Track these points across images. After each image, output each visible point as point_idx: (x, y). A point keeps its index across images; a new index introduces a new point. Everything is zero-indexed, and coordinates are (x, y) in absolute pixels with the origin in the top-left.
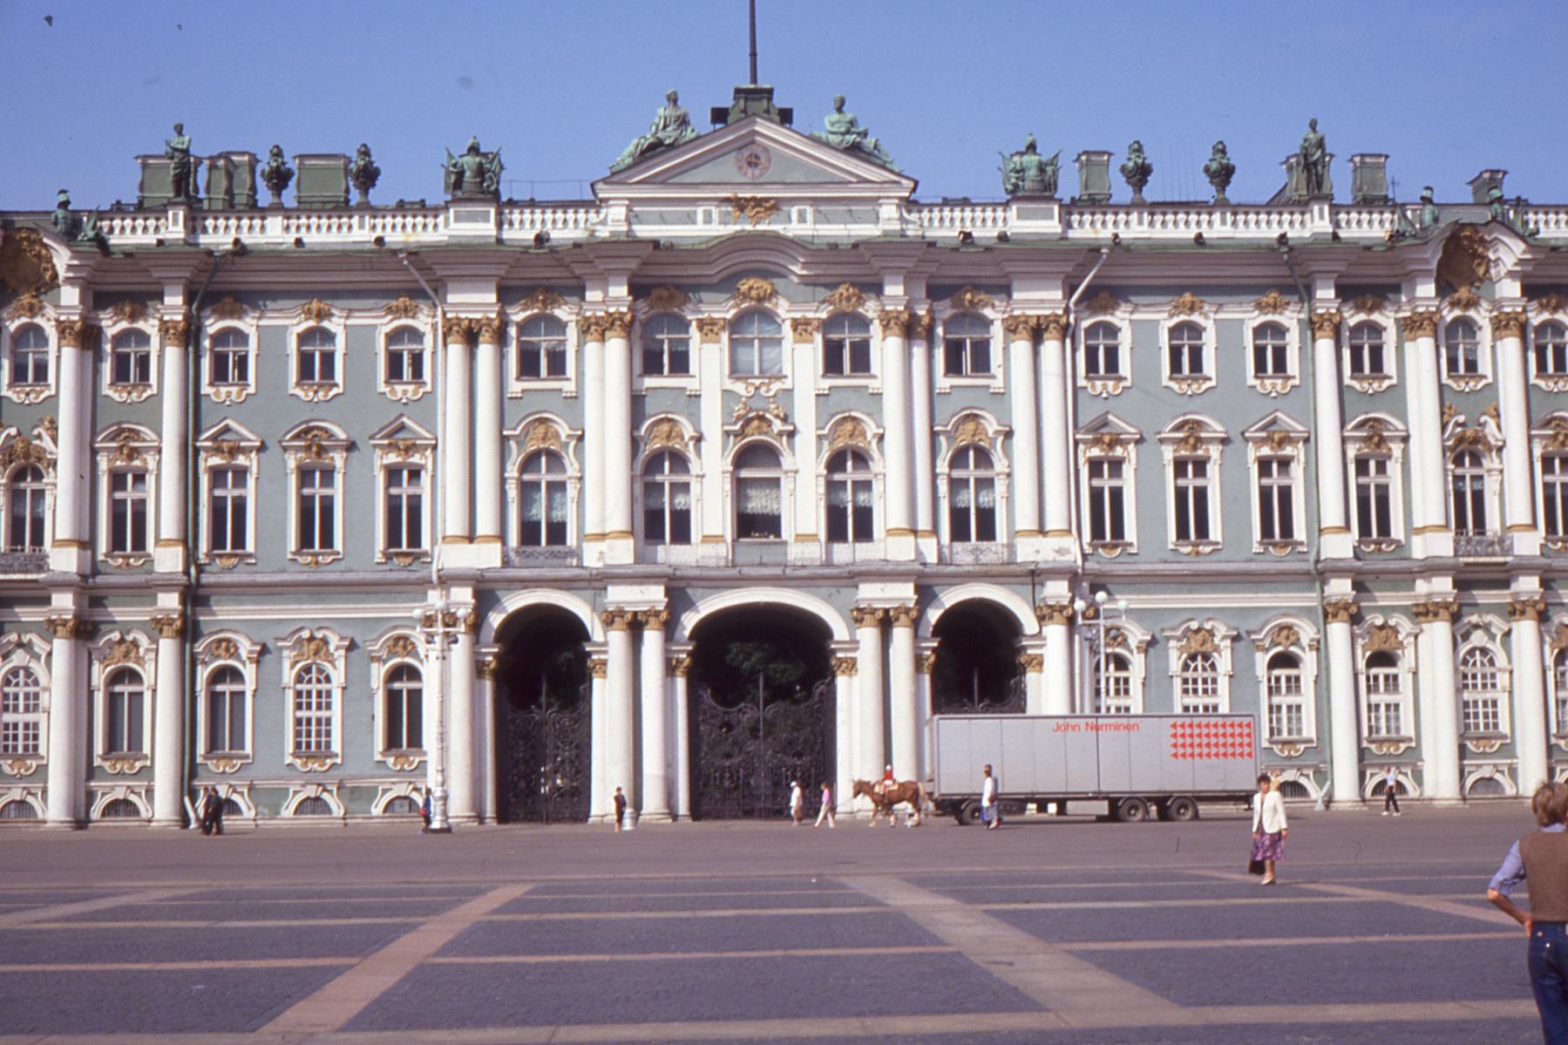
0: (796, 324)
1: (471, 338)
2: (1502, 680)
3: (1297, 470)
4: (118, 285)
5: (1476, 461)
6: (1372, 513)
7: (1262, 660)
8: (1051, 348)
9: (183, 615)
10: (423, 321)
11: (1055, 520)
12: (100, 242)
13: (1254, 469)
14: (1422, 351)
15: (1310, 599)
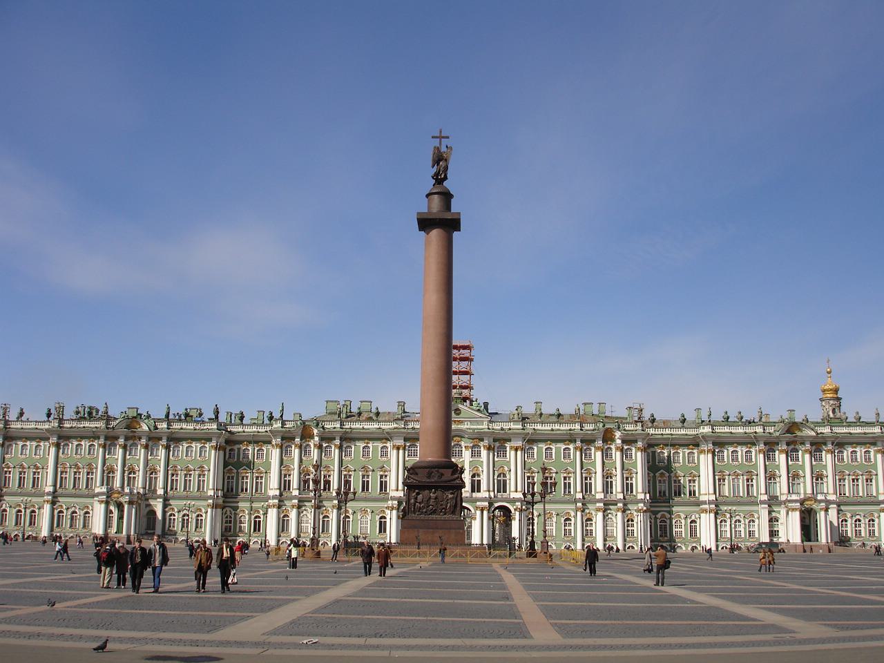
0: (465, 447)
1: (398, 449)
2: (615, 525)
3: (572, 479)
4: (327, 438)
5: (611, 478)
6: (587, 488)
7: (563, 519)
8: (519, 453)
9: (338, 505)
10: (388, 445)
11: (519, 489)
12: (323, 428)
13: (563, 479)
14: (599, 454)
15: (573, 507)
